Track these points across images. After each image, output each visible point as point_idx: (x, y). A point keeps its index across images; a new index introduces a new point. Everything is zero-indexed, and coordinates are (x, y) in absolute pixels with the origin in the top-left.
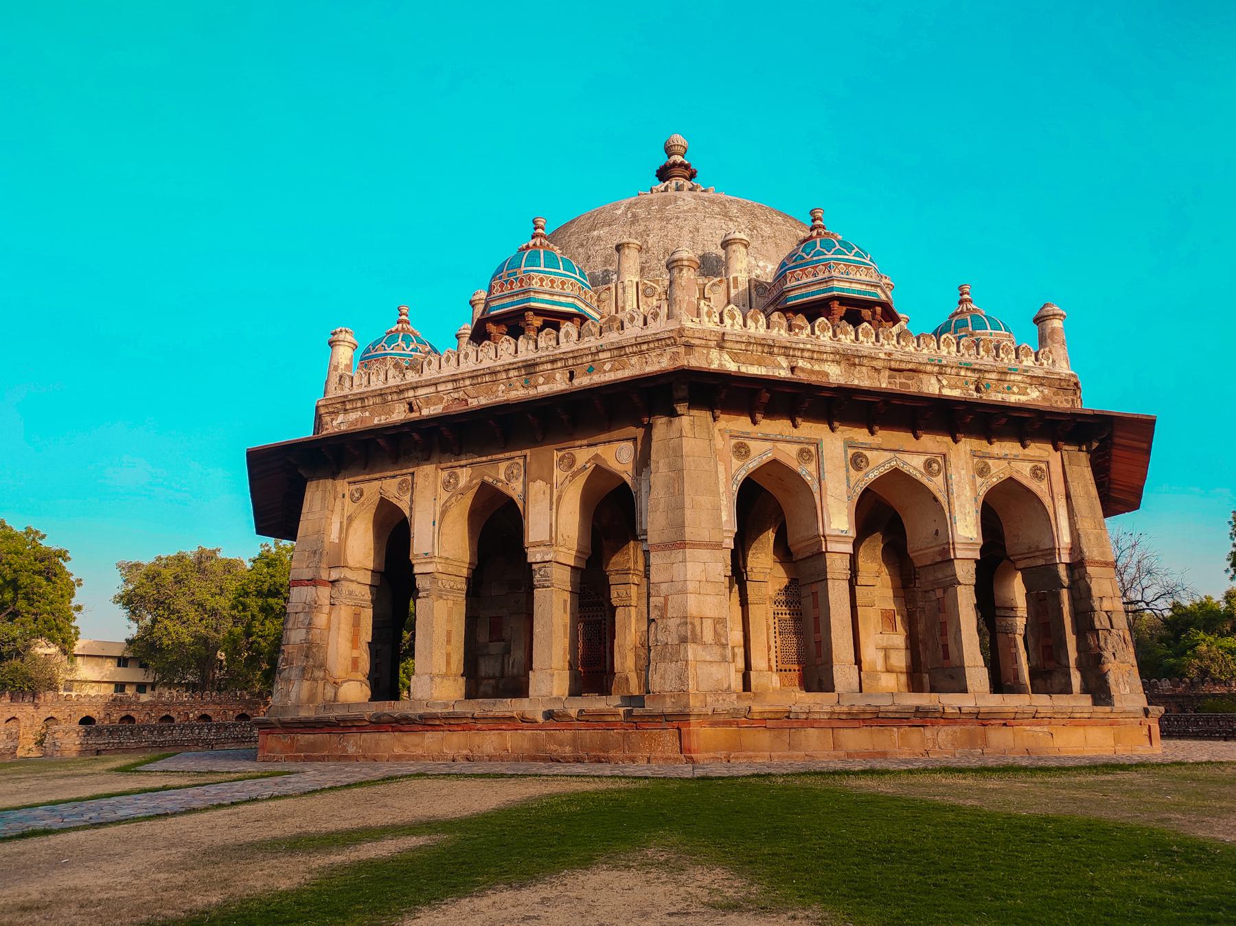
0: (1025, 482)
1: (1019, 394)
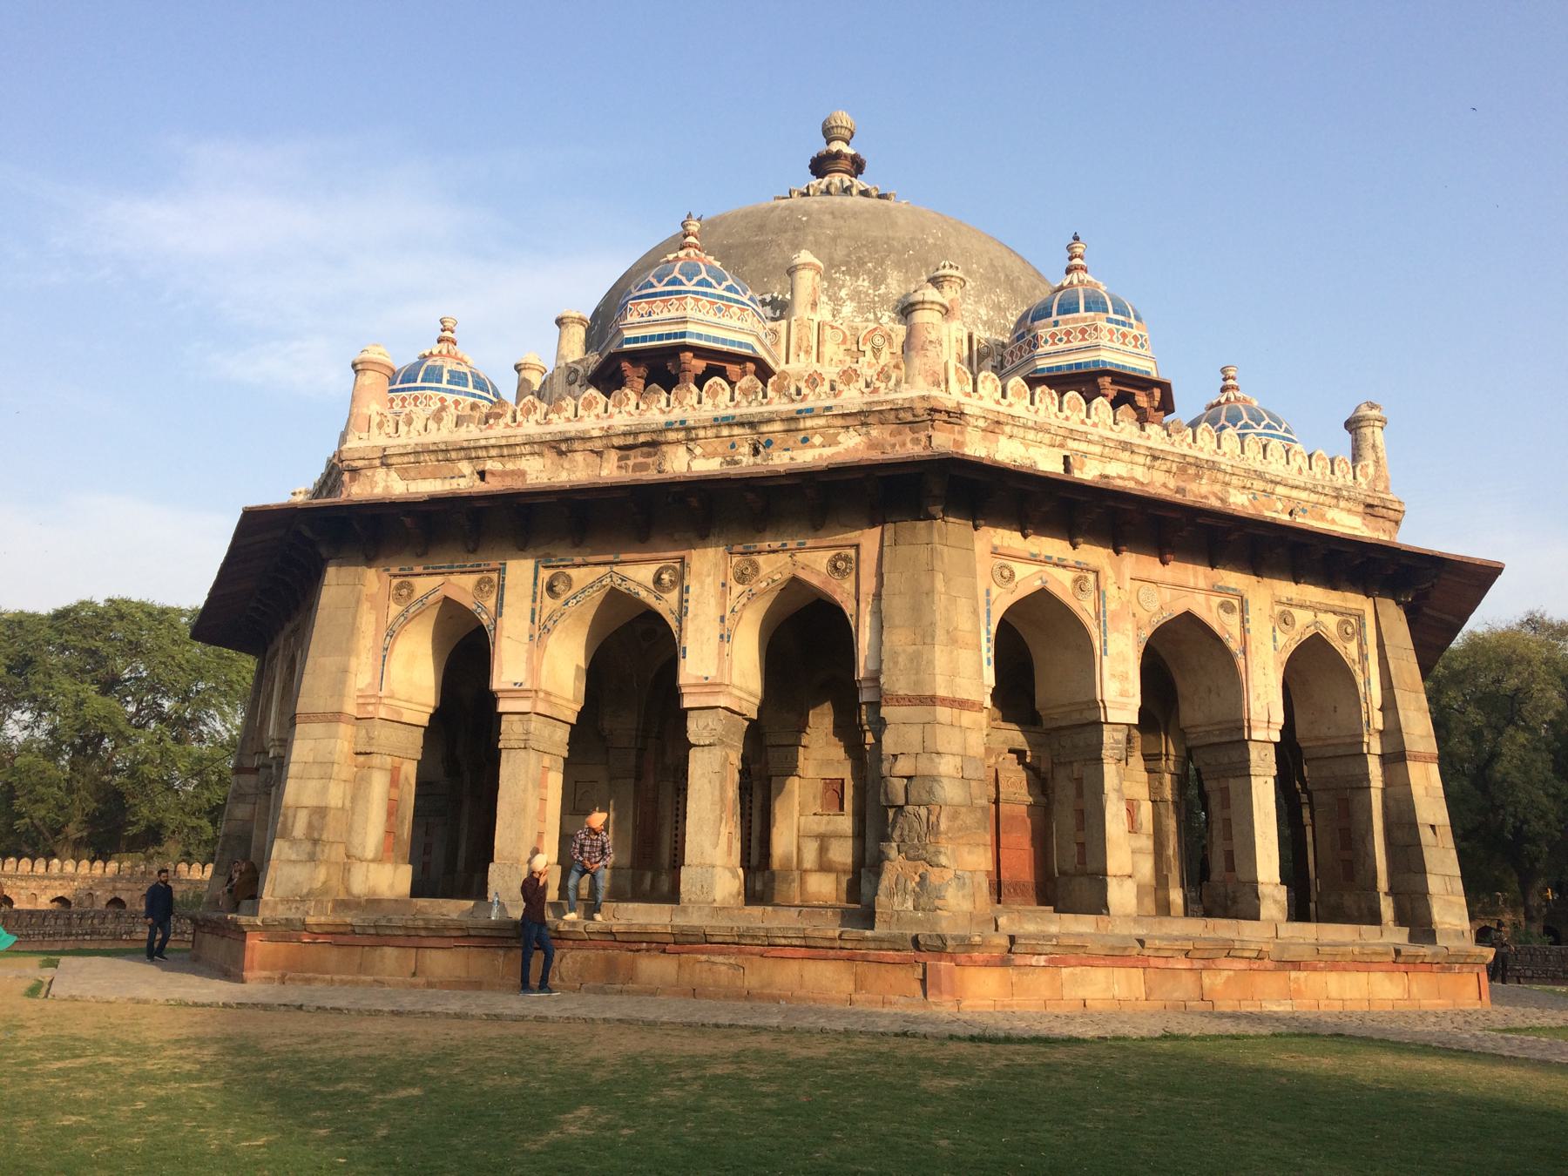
0: (815, 581)
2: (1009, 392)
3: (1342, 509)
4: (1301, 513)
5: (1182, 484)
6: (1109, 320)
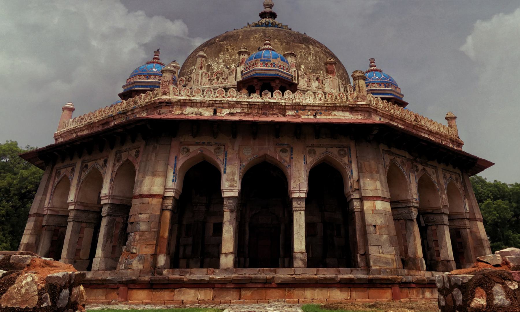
4: (319, 114)
6: (261, 61)
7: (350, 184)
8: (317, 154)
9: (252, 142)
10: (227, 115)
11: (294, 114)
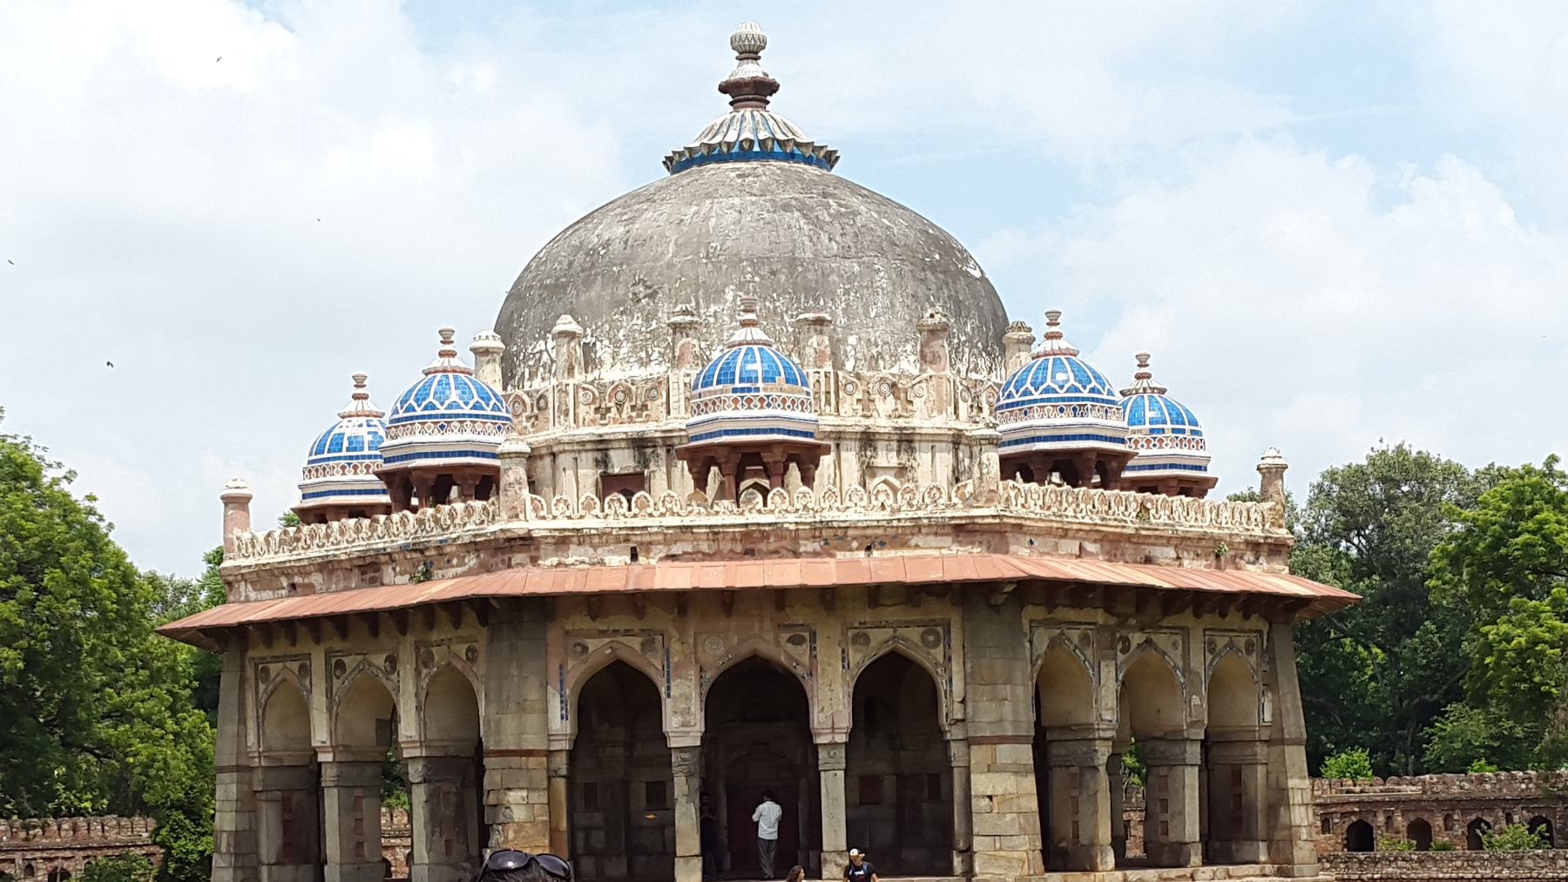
1: (457, 566)
2: (580, 507)
3: (927, 534)
5: (750, 546)
6: (735, 390)
7: (950, 707)
8: (873, 643)
9: (722, 623)
10: (661, 559)
11: (818, 549)
